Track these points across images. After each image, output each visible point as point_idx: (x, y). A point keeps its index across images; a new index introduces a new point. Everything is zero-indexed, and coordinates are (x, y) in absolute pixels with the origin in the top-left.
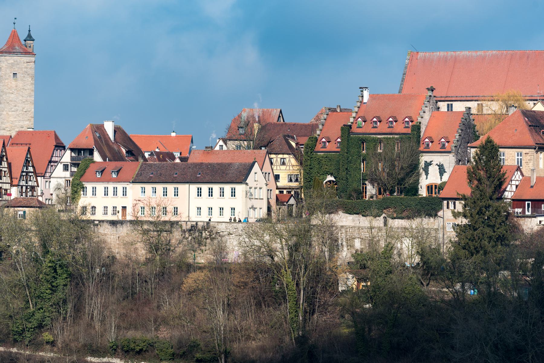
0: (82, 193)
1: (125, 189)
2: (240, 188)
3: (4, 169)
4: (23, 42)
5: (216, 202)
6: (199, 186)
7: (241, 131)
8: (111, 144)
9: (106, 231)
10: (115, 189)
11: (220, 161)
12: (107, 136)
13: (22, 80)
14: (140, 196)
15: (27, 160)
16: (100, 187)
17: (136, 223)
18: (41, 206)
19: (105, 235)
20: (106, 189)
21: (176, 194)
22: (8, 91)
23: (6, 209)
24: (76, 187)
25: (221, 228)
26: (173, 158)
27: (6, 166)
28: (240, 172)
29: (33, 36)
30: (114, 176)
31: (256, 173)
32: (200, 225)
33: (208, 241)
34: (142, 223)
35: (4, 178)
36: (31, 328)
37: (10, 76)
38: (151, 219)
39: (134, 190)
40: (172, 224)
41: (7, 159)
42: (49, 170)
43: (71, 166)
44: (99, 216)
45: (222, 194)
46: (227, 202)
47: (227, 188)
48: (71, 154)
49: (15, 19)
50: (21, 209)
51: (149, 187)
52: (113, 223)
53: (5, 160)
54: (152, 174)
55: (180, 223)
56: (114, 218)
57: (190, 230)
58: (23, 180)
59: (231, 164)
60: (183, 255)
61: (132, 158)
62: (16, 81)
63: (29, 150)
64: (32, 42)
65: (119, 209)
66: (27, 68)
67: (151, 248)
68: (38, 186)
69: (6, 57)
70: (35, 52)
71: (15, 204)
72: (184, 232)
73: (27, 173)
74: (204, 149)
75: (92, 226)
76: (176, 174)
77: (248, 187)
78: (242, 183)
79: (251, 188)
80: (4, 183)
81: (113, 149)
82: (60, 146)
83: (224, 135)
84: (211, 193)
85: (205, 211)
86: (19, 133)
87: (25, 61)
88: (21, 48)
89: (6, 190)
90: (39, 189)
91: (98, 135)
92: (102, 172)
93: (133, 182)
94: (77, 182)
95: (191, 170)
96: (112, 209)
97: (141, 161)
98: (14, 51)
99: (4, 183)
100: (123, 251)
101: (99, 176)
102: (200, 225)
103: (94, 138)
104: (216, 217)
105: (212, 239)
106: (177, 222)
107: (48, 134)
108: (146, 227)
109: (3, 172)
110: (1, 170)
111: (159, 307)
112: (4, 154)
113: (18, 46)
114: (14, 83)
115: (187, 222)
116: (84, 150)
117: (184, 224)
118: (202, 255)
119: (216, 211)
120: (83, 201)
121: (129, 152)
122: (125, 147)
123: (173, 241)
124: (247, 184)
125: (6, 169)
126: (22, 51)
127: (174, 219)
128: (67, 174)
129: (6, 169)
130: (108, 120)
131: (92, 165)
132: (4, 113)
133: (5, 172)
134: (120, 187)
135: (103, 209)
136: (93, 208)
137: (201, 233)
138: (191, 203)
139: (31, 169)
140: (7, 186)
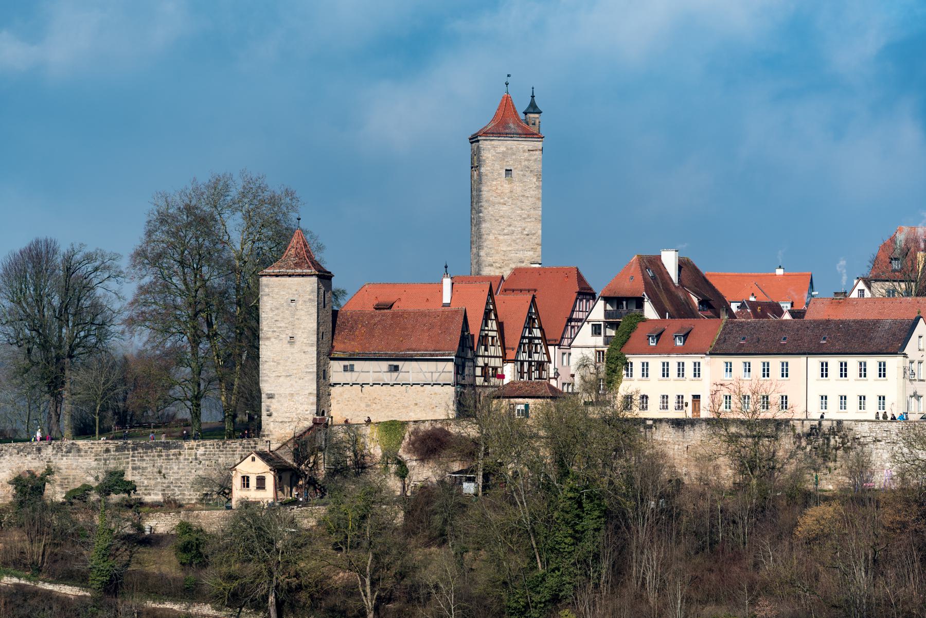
0: (624, 372)
1: (697, 366)
2: (894, 363)
3: (491, 334)
4: (522, 116)
5: (853, 386)
6: (824, 359)
7: (896, 265)
8: (673, 289)
9: (665, 436)
10: (681, 366)
11: (859, 316)
12: (666, 276)
13: (520, 181)
14: (723, 376)
15: (530, 318)
16: (656, 363)
17: (716, 423)
18: (555, 395)
19: (665, 443)
20: (666, 366)
21: (785, 374)
22: (496, 200)
23: (495, 401)
24: (614, 363)
25: (862, 430)
26: (780, 312)
27: (495, 328)
28: (894, 334)
29: (540, 107)
31: (920, 337)
33: (840, 453)
34: (727, 422)
35: (492, 348)
36: (540, 603)
37: (499, 174)
38: (741, 416)
39: (713, 367)
40: (779, 424)
41: (496, 315)
42: (568, 335)
43: (605, 327)
44: (654, 411)
45: (863, 372)
46: (872, 386)
47: (872, 362)
48: (605, 307)
49: (509, 76)
50: (521, 400)
51: (738, 362)
52: (678, 424)
53: (493, 317)
54: (744, 339)
55: (791, 422)
56: (680, 415)
57: (809, 435)
58: (524, 352)
59: (878, 321)
60: (797, 476)
61: (709, 313)
64: (537, 115)
65: (688, 399)
66: (529, 160)
67: (743, 465)
68: (549, 361)
69: (493, 142)
70: (543, 133)
72: (798, 437)
74: (833, 296)
75: (642, 429)
76: (785, 339)
77: (908, 360)
78: (896, 353)
79: (912, 362)
80: (491, 357)
81: (677, 297)
82: (587, 294)
83: (866, 271)
84: (844, 372)
85: (833, 402)
86: (517, 272)
87: (526, 148)
88: (518, 126)
89: (495, 369)
90: (551, 366)
91: (651, 274)
92: (658, 336)
93: (711, 354)
94: (615, 354)
97: (725, 317)
98: (507, 131)
99: (491, 357)
100: (694, 471)
103: (644, 279)
104: (852, 413)
105: (847, 450)
106: (787, 421)
108: (733, 429)
109: (490, 339)
110: (487, 335)
111: (756, 566)
112: (491, 307)
113: (514, 123)
114: (507, 186)
115: (803, 421)
116: (628, 299)
117: (798, 424)
118: (829, 476)
119: (853, 402)
120: (626, 387)
121: (704, 303)
122: (697, 294)
123: (780, 454)
124: (905, 356)
125: (494, 334)
126: (520, 132)
127: (781, 415)
128: (599, 341)
129: (494, 334)
130: (668, 248)
131: (641, 325)
132: (491, 237)
133: (493, 337)
134: (689, 362)
135: (660, 400)
136: (644, 397)
137: (827, 440)
138: (810, 389)
139: (537, 333)
140: (497, 362)
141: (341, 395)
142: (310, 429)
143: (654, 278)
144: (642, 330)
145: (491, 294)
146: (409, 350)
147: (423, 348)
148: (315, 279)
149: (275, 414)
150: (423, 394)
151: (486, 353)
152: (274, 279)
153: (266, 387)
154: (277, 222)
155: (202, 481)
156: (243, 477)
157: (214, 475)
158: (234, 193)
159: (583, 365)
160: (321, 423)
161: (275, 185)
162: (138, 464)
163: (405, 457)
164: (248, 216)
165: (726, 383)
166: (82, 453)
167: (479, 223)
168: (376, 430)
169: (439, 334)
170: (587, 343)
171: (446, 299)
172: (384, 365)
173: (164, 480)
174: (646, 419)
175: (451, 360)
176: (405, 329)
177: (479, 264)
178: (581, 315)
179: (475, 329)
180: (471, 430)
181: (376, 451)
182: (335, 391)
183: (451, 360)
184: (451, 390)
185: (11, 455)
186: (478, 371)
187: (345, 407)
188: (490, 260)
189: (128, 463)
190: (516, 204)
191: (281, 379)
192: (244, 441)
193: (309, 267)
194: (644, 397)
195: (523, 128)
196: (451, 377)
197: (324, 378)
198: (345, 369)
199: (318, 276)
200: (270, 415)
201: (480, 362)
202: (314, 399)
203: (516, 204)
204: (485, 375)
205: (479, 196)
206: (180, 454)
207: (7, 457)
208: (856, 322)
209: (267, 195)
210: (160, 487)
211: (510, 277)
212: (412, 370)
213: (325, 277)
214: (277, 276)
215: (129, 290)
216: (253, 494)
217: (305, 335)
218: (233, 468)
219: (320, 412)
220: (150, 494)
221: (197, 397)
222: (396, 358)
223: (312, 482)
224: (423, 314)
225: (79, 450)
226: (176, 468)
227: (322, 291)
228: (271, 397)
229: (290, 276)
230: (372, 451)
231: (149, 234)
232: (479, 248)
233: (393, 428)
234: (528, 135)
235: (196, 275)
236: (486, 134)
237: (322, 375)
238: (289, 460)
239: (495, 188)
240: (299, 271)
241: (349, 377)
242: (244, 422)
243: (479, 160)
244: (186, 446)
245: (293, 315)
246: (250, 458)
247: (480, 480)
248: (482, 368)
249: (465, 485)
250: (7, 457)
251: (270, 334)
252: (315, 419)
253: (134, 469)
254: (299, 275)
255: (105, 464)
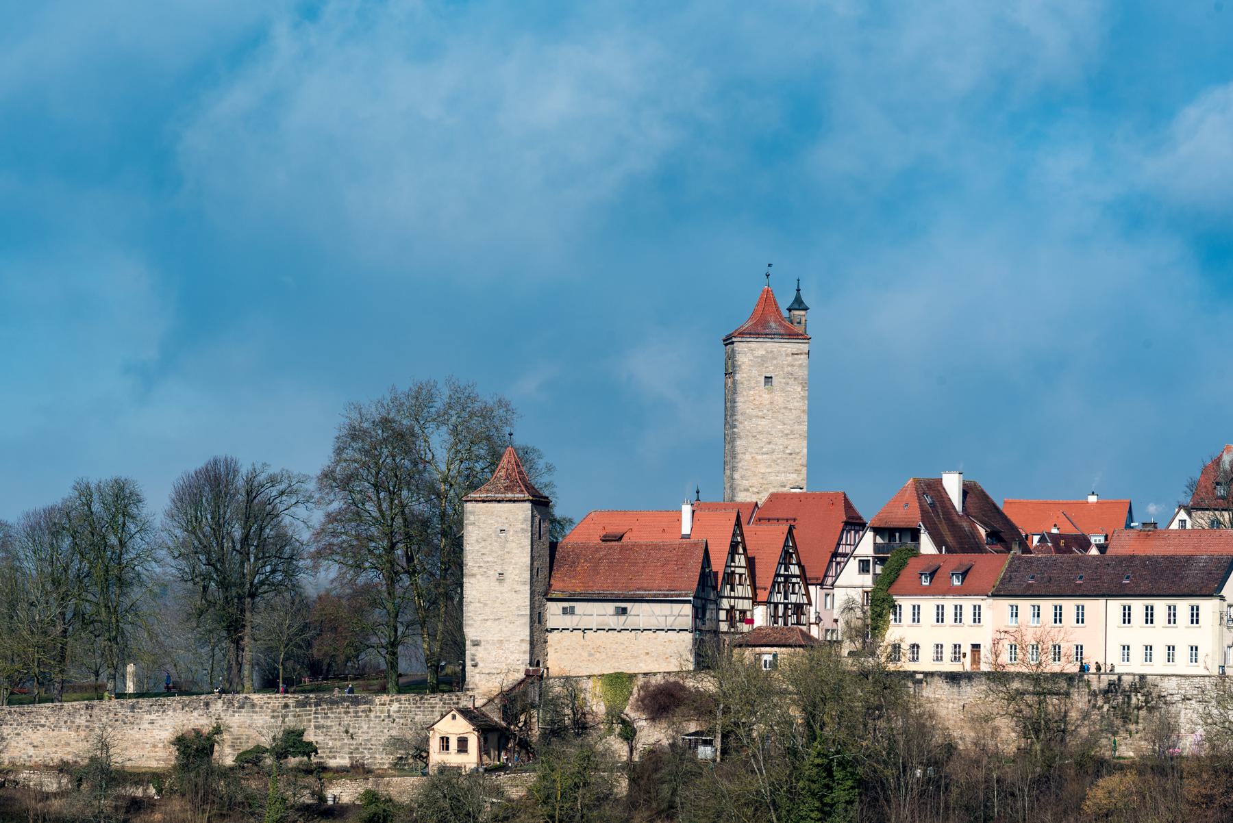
0: (892, 617)
1: (977, 611)
2: (1208, 607)
3: (738, 570)
4: (786, 314)
5: (1160, 634)
7: (1220, 491)
8: (956, 518)
9: (936, 692)
10: (958, 610)
11: (1170, 551)
12: (948, 503)
13: (782, 390)
15: (787, 552)
16: (928, 606)
17: (998, 677)
18: (807, 642)
19: (937, 701)
20: (940, 610)
21: (1080, 619)
23: (737, 650)
24: (880, 606)
25: (1169, 686)
26: (1085, 544)
27: (743, 564)
30: (956, 582)
32: (1127, 680)
33: (1143, 713)
35: (740, 588)
37: (757, 382)
38: (1025, 670)
39: (996, 611)
41: (745, 549)
42: (832, 572)
43: (875, 563)
44: (926, 663)
46: (1183, 634)
47: (1183, 606)
51: (1025, 605)
53: (741, 551)
56: (956, 668)
57: (1106, 692)
59: (1191, 557)
60: (1092, 741)
61: (999, 547)
62: (771, 391)
63: (790, 532)
64: (802, 313)
65: (966, 649)
68: (810, 604)
70: (809, 334)
71: (760, 639)
72: (1094, 694)
73: (787, 577)
75: (910, 684)
77: (1225, 604)
81: (961, 529)
84: (1149, 617)
85: (1137, 653)
86: (774, 497)
87: (789, 351)
88: (781, 325)
89: (743, 612)
90: (812, 609)
92: (932, 575)
93: (993, 595)
94: (881, 595)
95: (1110, 570)
96: (951, 649)
101: (925, 583)
102: (1127, 680)
103: (921, 506)
104: (1159, 665)
105: (1151, 710)
107: (830, 499)
108: (1016, 685)
110: (733, 572)
114: (766, 396)
116: (902, 531)
117: (1094, 679)
118: (1129, 741)
119: (1160, 653)
120: (894, 633)
121: (994, 535)
122: (984, 524)
123: (1073, 715)
124: (1222, 598)
125: (742, 571)
128: (867, 580)
130: (950, 470)
131: (912, 562)
132: (748, 457)
133: (741, 575)
134: (968, 604)
135: (933, 649)
136: (915, 647)
137: (1130, 698)
139: (794, 570)
140: (746, 605)
141: (559, 642)
142: (523, 681)
143: (933, 505)
144: (913, 566)
145: (738, 523)
146: (639, 589)
147: (655, 586)
148: (528, 505)
149: (481, 665)
150: (655, 641)
151: (732, 594)
152: (481, 504)
153: (470, 633)
154: (489, 438)
155: (396, 743)
156: (442, 738)
157: (409, 735)
158: (439, 404)
159: (849, 608)
160: (535, 675)
161: (486, 395)
162: (322, 721)
163: (633, 715)
164: (455, 431)
165: (1011, 630)
166: (257, 709)
167: (733, 441)
168: (599, 684)
169: (674, 571)
170: (853, 582)
171: (686, 529)
172: (610, 607)
173: (351, 741)
174: (915, 672)
175: (689, 602)
176: (635, 564)
177: (732, 488)
178: (848, 549)
179: (718, 565)
180: (708, 684)
181: (598, 707)
182: (551, 637)
183: (689, 602)
184: (688, 637)
185: (175, 710)
186: (723, 615)
187: (562, 658)
188: (745, 483)
189: (310, 721)
190: (776, 418)
191: (489, 623)
192: (446, 696)
193: (522, 491)
194: (915, 647)
195: (786, 328)
196: (688, 622)
197: (540, 622)
198: (565, 611)
199: (532, 501)
200: (475, 666)
201: (725, 604)
202: (527, 647)
203: (776, 418)
204: (731, 619)
205: (733, 408)
206: (370, 711)
207: (170, 713)
208: (1163, 557)
209: (477, 406)
210: (347, 750)
211: (765, 504)
212: (642, 613)
213: (541, 503)
214: (484, 501)
215: (317, 517)
216: (453, 758)
217: (517, 572)
218: (430, 727)
219: (534, 662)
220: (335, 757)
221: (393, 644)
222: (623, 599)
223: (524, 745)
224: (656, 547)
225: (253, 706)
226: (365, 727)
227: (537, 520)
228: (476, 644)
229: (499, 501)
230: (594, 708)
231: (339, 451)
232: (733, 469)
233: (618, 682)
234: (792, 335)
235: (392, 500)
236: (742, 334)
237: (537, 618)
238: (496, 717)
239: (752, 398)
240: (510, 495)
241: (568, 621)
242: (445, 675)
243: (734, 366)
244: (377, 701)
245: (503, 547)
246: (450, 716)
247: (718, 744)
248: (728, 611)
249: (701, 749)
250: (170, 713)
251: (475, 570)
252: (527, 671)
253: (316, 727)
254: (510, 501)
255: (283, 722)
